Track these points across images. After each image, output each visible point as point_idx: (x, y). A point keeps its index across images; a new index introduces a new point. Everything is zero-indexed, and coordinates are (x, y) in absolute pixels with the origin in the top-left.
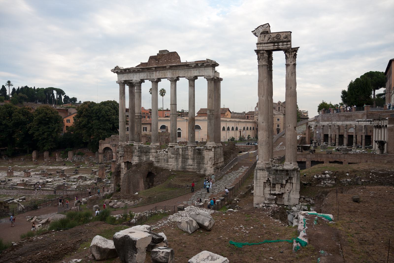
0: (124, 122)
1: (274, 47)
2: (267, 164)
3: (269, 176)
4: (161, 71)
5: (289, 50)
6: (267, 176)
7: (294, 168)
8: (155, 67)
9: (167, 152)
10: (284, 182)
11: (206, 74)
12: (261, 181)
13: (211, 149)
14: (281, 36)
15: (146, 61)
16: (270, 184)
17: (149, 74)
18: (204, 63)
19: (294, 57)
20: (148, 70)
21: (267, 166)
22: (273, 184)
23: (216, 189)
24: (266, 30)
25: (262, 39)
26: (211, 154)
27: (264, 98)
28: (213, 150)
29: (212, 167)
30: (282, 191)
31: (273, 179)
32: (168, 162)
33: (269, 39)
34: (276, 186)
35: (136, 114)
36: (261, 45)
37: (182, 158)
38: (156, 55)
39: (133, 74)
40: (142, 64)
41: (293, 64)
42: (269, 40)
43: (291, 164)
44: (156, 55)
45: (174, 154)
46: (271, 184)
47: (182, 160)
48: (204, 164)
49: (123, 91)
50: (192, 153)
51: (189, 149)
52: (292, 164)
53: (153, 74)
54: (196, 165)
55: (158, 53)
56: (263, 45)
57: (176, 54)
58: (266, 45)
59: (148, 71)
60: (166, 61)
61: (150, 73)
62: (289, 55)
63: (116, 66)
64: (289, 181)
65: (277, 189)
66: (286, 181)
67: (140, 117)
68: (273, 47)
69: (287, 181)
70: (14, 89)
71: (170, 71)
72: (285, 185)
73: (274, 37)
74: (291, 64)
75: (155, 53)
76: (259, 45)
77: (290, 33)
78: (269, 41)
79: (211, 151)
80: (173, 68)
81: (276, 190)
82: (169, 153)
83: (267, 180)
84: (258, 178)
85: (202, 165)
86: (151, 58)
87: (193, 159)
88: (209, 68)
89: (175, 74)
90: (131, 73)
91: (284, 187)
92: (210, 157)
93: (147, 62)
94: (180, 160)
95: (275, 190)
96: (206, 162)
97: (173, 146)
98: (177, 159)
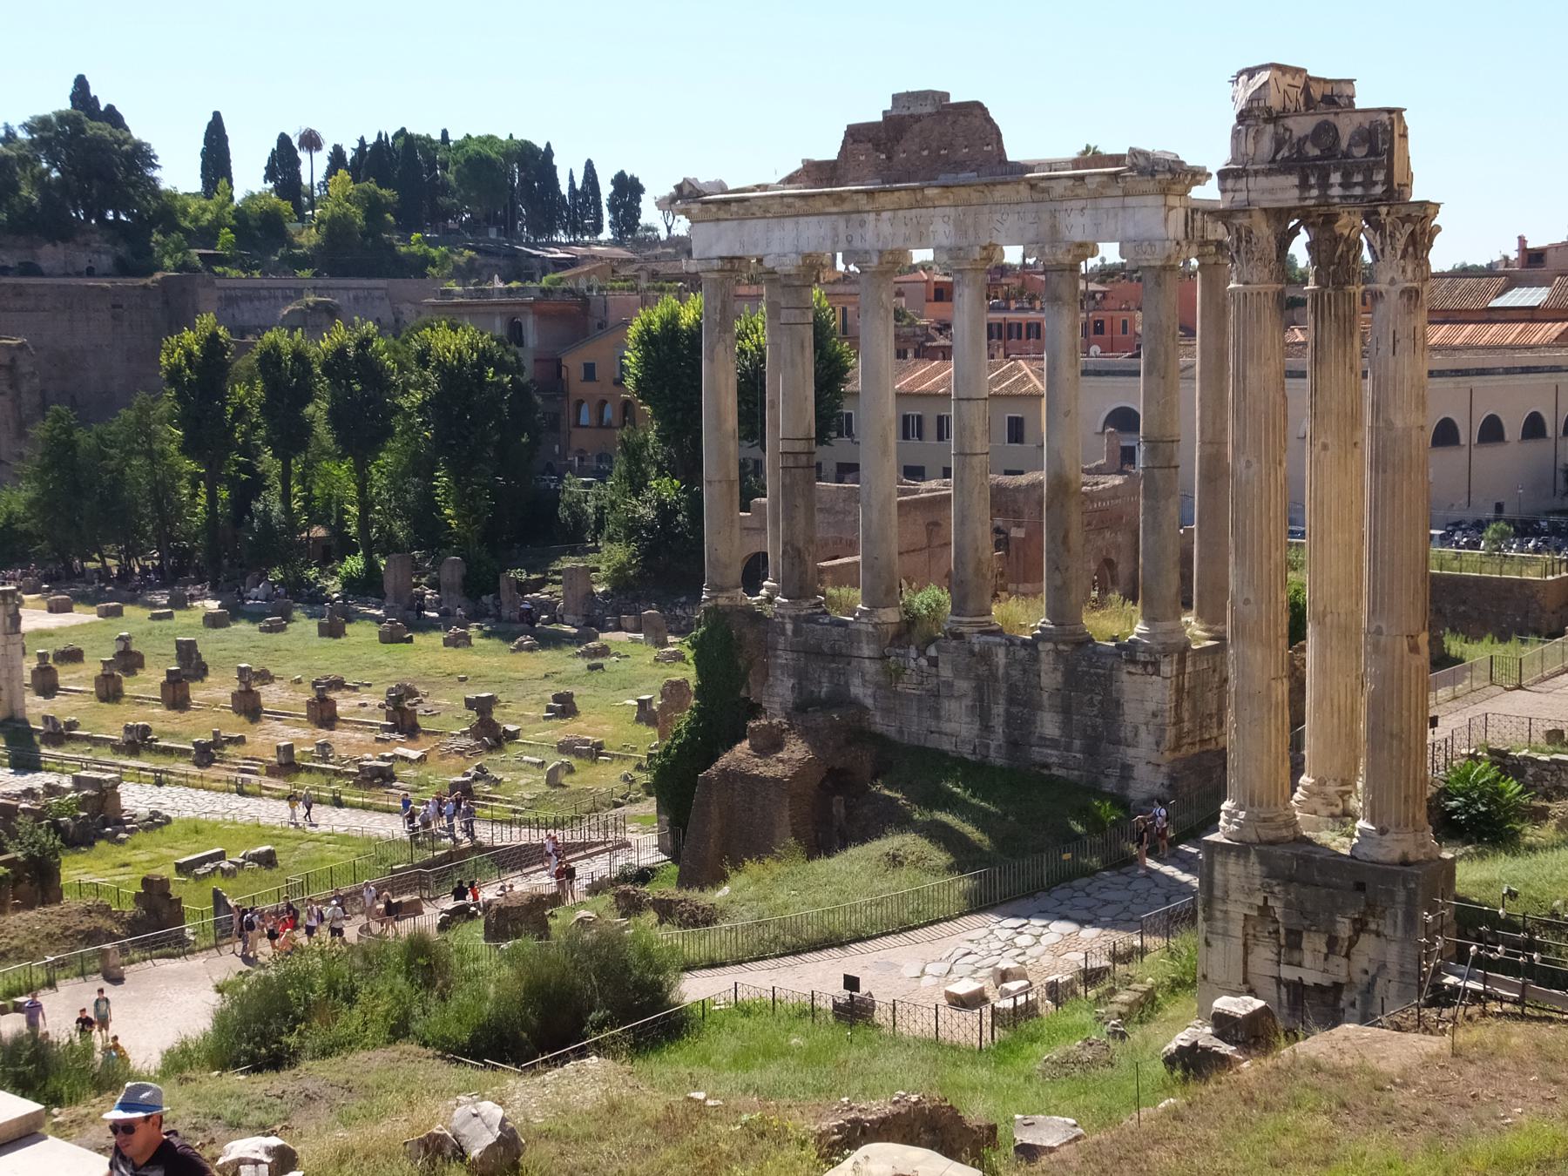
0: (730, 483)
3: (1269, 885)
4: (901, 213)
6: (1258, 881)
7: (1396, 855)
9: (933, 662)
10: (1344, 928)
12: (1230, 907)
13: (1156, 664)
15: (829, 150)
16: (1277, 932)
18: (1116, 174)
19: (1410, 249)
22: (1289, 932)
23: (1114, 902)
24: (1262, 104)
28: (1167, 669)
30: (1339, 970)
31: (1288, 905)
32: (938, 717)
33: (1277, 152)
34: (1305, 944)
36: (1242, 184)
37: (1011, 701)
38: (880, 118)
39: (763, 222)
40: (815, 172)
41: (1402, 292)
42: (1285, 153)
44: (880, 118)
45: (967, 678)
46: (1282, 930)
47: (1007, 711)
50: (1059, 676)
51: (1043, 655)
52: (1387, 837)
53: (862, 224)
54: (1077, 743)
56: (1251, 180)
57: (978, 111)
58: (1263, 182)
59: (835, 209)
60: (925, 153)
61: (847, 222)
62: (1383, 236)
63: (680, 181)
64: (1373, 926)
65: (1308, 958)
66: (1354, 921)
68: (1296, 192)
69: (1360, 927)
70: (337, 156)
71: (951, 211)
72: (1352, 942)
75: (873, 111)
76: (1230, 183)
77: (1385, 117)
78: (1279, 157)
79: (1157, 673)
80: (963, 192)
82: (946, 672)
84: (1218, 893)
86: (855, 134)
87: (1066, 710)
88: (1150, 200)
89: (971, 231)
90: (753, 216)
91: (1347, 956)
92: (1151, 706)
93: (834, 157)
94: (999, 710)
95: (1300, 965)
96: (1126, 732)
97: (965, 629)
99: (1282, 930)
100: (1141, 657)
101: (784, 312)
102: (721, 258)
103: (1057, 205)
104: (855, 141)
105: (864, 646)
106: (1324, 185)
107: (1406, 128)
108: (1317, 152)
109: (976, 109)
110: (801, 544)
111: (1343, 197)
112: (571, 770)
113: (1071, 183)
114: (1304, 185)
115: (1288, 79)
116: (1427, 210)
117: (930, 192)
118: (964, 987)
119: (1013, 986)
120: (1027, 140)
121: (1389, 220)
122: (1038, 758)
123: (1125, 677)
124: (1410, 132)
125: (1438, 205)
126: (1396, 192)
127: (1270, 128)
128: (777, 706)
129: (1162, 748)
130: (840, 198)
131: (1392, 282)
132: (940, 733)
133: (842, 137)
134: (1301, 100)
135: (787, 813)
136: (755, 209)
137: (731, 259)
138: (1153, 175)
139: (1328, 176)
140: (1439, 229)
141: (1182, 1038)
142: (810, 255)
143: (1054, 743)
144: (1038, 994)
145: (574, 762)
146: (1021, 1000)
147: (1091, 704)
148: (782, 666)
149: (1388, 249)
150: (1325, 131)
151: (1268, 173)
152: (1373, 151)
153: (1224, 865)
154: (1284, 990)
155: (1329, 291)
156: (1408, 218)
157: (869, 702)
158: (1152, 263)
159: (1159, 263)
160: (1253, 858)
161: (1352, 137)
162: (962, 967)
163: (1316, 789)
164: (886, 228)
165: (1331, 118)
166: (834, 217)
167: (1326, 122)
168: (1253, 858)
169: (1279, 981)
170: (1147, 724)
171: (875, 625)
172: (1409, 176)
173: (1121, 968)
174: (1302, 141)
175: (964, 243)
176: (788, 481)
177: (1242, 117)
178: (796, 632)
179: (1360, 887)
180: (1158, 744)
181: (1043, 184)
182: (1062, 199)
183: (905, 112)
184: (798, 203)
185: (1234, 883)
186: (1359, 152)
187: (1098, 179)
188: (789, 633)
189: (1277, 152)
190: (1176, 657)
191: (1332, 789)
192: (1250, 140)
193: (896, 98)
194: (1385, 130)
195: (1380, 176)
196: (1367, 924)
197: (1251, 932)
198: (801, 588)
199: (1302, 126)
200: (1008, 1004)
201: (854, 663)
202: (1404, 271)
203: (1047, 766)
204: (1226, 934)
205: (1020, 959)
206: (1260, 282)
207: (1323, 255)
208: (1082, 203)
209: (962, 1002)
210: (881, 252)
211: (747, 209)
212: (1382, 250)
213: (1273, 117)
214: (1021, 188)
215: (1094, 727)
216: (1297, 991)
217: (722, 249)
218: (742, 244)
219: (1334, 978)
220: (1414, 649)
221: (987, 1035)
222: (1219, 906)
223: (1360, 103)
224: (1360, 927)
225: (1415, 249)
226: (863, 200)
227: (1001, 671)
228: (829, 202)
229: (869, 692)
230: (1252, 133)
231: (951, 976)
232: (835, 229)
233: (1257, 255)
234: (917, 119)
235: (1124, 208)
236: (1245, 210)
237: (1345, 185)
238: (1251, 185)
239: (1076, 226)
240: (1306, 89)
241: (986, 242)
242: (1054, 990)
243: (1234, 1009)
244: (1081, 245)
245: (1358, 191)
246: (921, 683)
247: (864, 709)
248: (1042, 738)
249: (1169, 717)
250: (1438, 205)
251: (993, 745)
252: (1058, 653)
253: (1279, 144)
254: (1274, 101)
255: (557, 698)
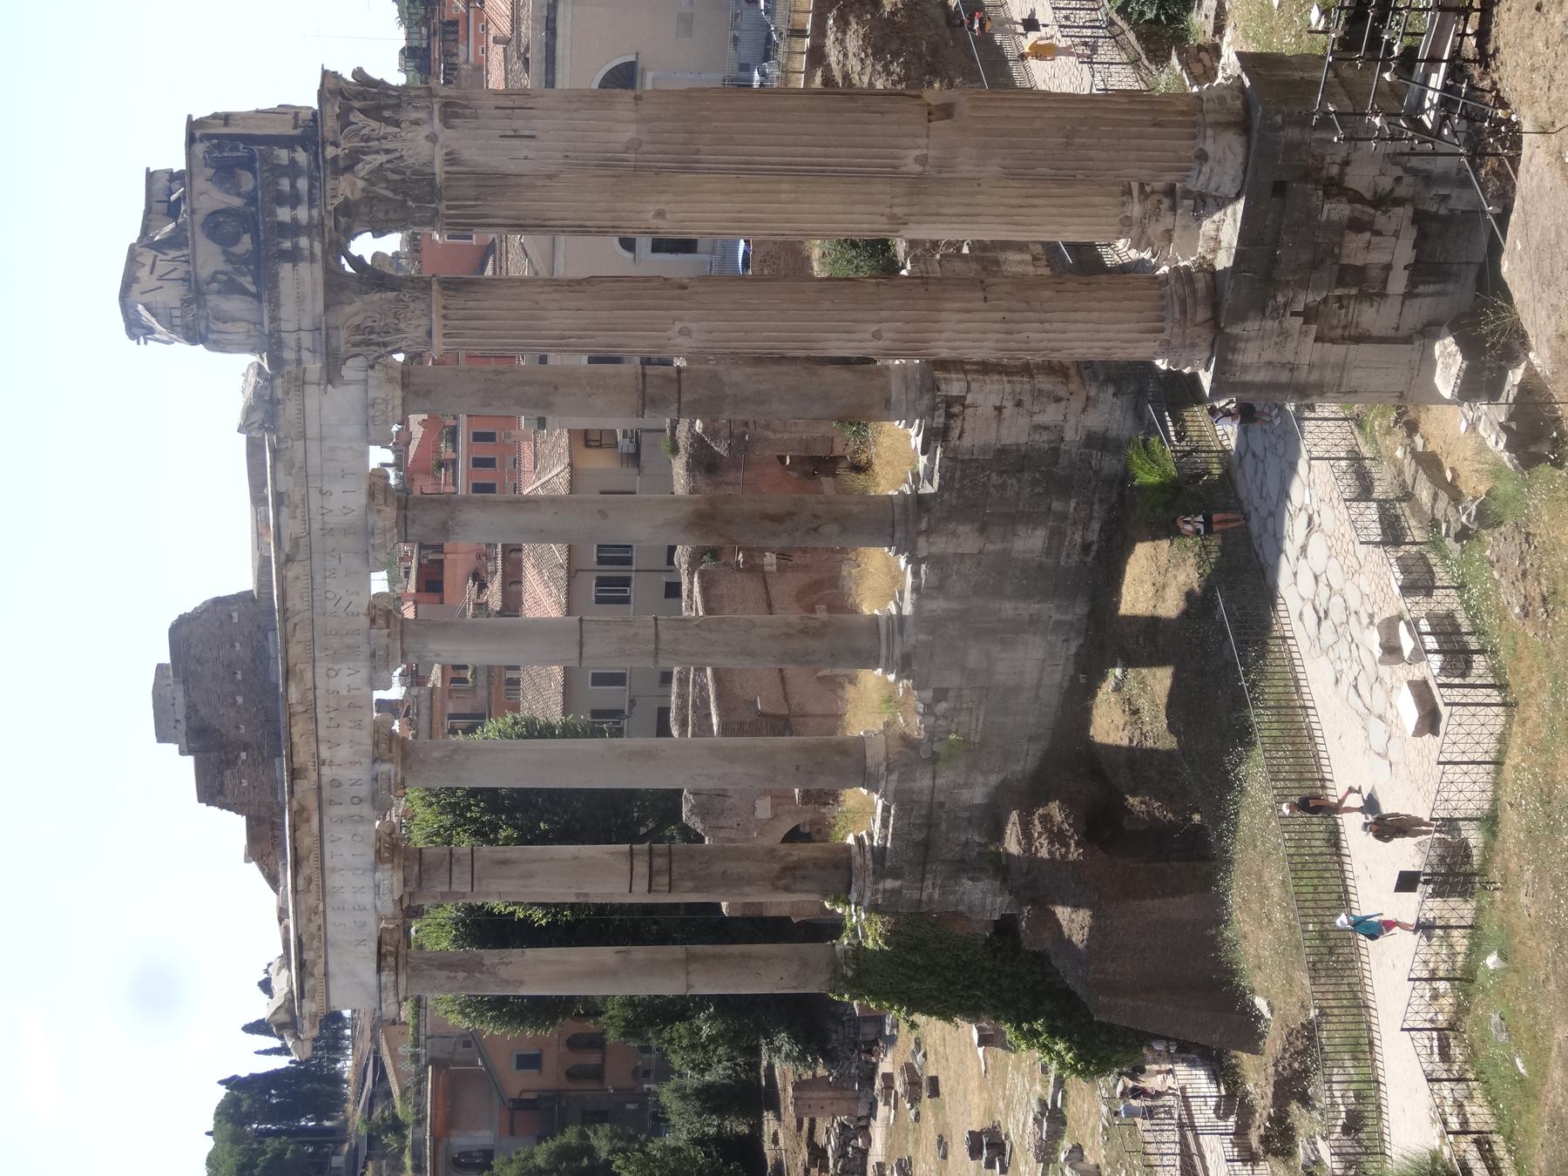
0: (690, 958)
1: (306, 253)
2: (1184, 312)
3: (1276, 309)
4: (322, 733)
5: (335, 159)
6: (1269, 324)
8: (294, 774)
9: (940, 695)
10: (1337, 210)
11: (354, 430)
12: (1305, 360)
13: (950, 402)
14: (222, 206)
15: (232, 827)
16: (1340, 298)
17: (336, 811)
18: (274, 452)
19: (386, 114)
20: (308, 821)
21: (1203, 314)
22: (1341, 282)
24: (177, 313)
25: (241, 338)
26: (986, 395)
27: (692, 326)
29: (1088, 398)
31: (1304, 285)
35: (641, 885)
36: (290, 339)
38: (190, 760)
40: (263, 846)
41: (447, 125)
43: (1202, 157)
44: (190, 760)
46: (1338, 292)
48: (1055, 451)
49: (461, 975)
50: (964, 529)
51: (934, 550)
53: (336, 784)
54: (1056, 505)
55: (174, 748)
56: (284, 326)
58: (288, 311)
60: (240, 700)
61: (331, 803)
64: (1335, 170)
65: (1377, 258)
66: (1327, 195)
67: (660, 862)
68: (303, 267)
71: (320, 671)
72: (1355, 197)
73: (225, 252)
74: (441, 139)
75: (181, 768)
78: (253, 289)
79: (960, 400)
80: (295, 650)
81: (1384, 258)
83: (1301, 320)
84: (1284, 377)
85: (1063, 461)
86: (211, 791)
87: (1012, 520)
88: (311, 404)
89: (349, 640)
90: (322, 928)
94: (1008, 608)
96: (1042, 439)
97: (897, 652)
98: (1008, 633)
99: (1338, 292)
100: (940, 421)
101: (455, 887)
102: (379, 970)
103: (316, 526)
104: (221, 792)
105: (917, 785)
106: (294, 229)
107: (215, 116)
108: (246, 239)
109: (182, 632)
110: (776, 866)
111: (311, 204)
112: (1077, 1150)
113: (285, 511)
114: (294, 256)
115: (143, 273)
116: (331, 85)
117: (294, 694)
118: (1408, 712)
119: (1407, 643)
120: (229, 568)
121: (343, 143)
122: (1076, 558)
123: (967, 442)
124: (221, 109)
125: (325, 73)
126: (305, 131)
127: (214, 300)
128: (999, 900)
129: (1063, 393)
130: (300, 815)
131: (432, 138)
132: (1039, 686)
133: (214, 810)
134: (173, 253)
135: (1148, 903)
136: (313, 928)
137: (381, 956)
138: (278, 402)
139: (281, 225)
140: (359, 73)
141: (1496, 443)
142: (378, 852)
143: (1056, 536)
144: (1419, 607)
145: (1066, 1144)
146: (1431, 643)
147: (1003, 486)
148: (943, 894)
149: (386, 145)
150: (218, 226)
151: (275, 304)
152: (248, 164)
153: (1245, 368)
154: (1421, 289)
155: (442, 207)
156: (344, 119)
157: (994, 780)
158: (398, 402)
159: (399, 393)
160: (1235, 330)
161: (227, 192)
162: (1378, 702)
163: (1135, 230)
164: (343, 753)
165: (199, 218)
166: (326, 820)
167: (203, 225)
168: (1235, 330)
169: (1409, 295)
170: (1031, 414)
171: (889, 770)
172: (283, 110)
173: (1379, 491)
174: (230, 258)
175: (365, 650)
176: (690, 884)
177: (194, 337)
178: (896, 877)
179: (1279, 188)
180: (1058, 400)
181: (287, 547)
182: (307, 520)
183: (183, 727)
184: (305, 871)
185: (1268, 355)
186: (247, 181)
187: (281, 475)
188: (897, 884)
189: (244, 292)
190: (938, 374)
191: (1136, 210)
192: (227, 327)
193: (162, 737)
194: (216, 147)
195: (283, 155)
196: (1331, 178)
197: (1339, 331)
198: (836, 867)
199: (209, 258)
200: (1436, 661)
201: (942, 798)
202: (416, 123)
203: (1086, 548)
204: (1342, 366)
205: (1365, 620)
206: (428, 315)
207: (392, 215)
208: (314, 494)
209: (1430, 721)
210: (375, 761)
211: (312, 937)
212: (387, 151)
213: (196, 291)
214: (290, 574)
215: (1035, 482)
216: (1421, 271)
217: (366, 969)
218: (362, 942)
219: (1406, 222)
220: (947, 111)
221: (1479, 695)
222: (1302, 376)
223: (179, 164)
224: (1335, 188)
225: (387, 107)
226: (303, 786)
227: (955, 605)
228: (304, 828)
229: (980, 779)
230: (221, 326)
231: (1390, 716)
232: (341, 820)
233: (391, 320)
234: (192, 708)
235: (321, 439)
236: (324, 331)
237: (293, 200)
238: (291, 326)
239: (346, 500)
240: (160, 247)
241: (364, 621)
242: (1418, 582)
243: (1454, 370)
244: (372, 495)
245: (303, 184)
246: (970, 710)
247: (1003, 786)
248: (1047, 552)
249: (1023, 385)
250: (325, 73)
251: (1056, 616)
252: (928, 532)
253: (232, 288)
254: (172, 295)
255: (975, 1152)
